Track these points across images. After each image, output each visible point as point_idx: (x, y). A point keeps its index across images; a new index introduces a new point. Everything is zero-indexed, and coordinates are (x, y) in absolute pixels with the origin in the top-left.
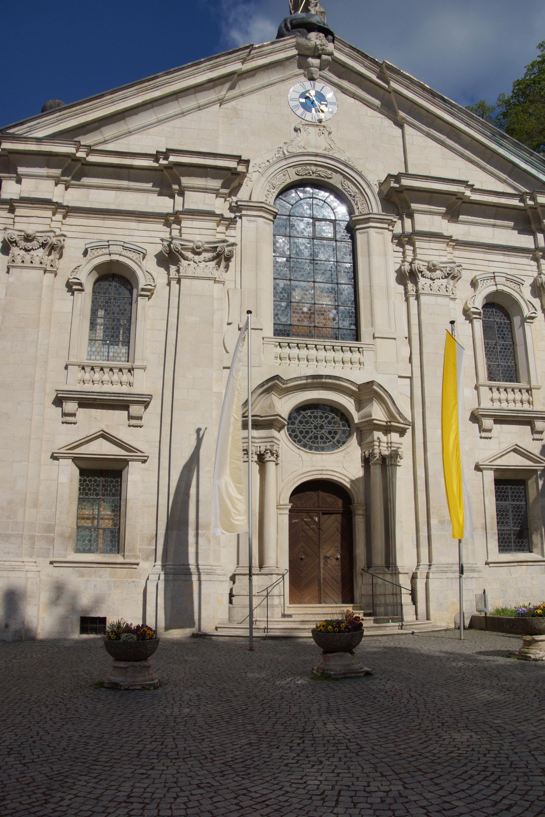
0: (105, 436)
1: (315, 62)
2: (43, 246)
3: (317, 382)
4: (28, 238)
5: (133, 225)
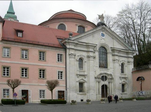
0: (82, 79)
1: (104, 29)
2: (74, 55)
3: (105, 73)
4: (72, 54)
5: (83, 52)
